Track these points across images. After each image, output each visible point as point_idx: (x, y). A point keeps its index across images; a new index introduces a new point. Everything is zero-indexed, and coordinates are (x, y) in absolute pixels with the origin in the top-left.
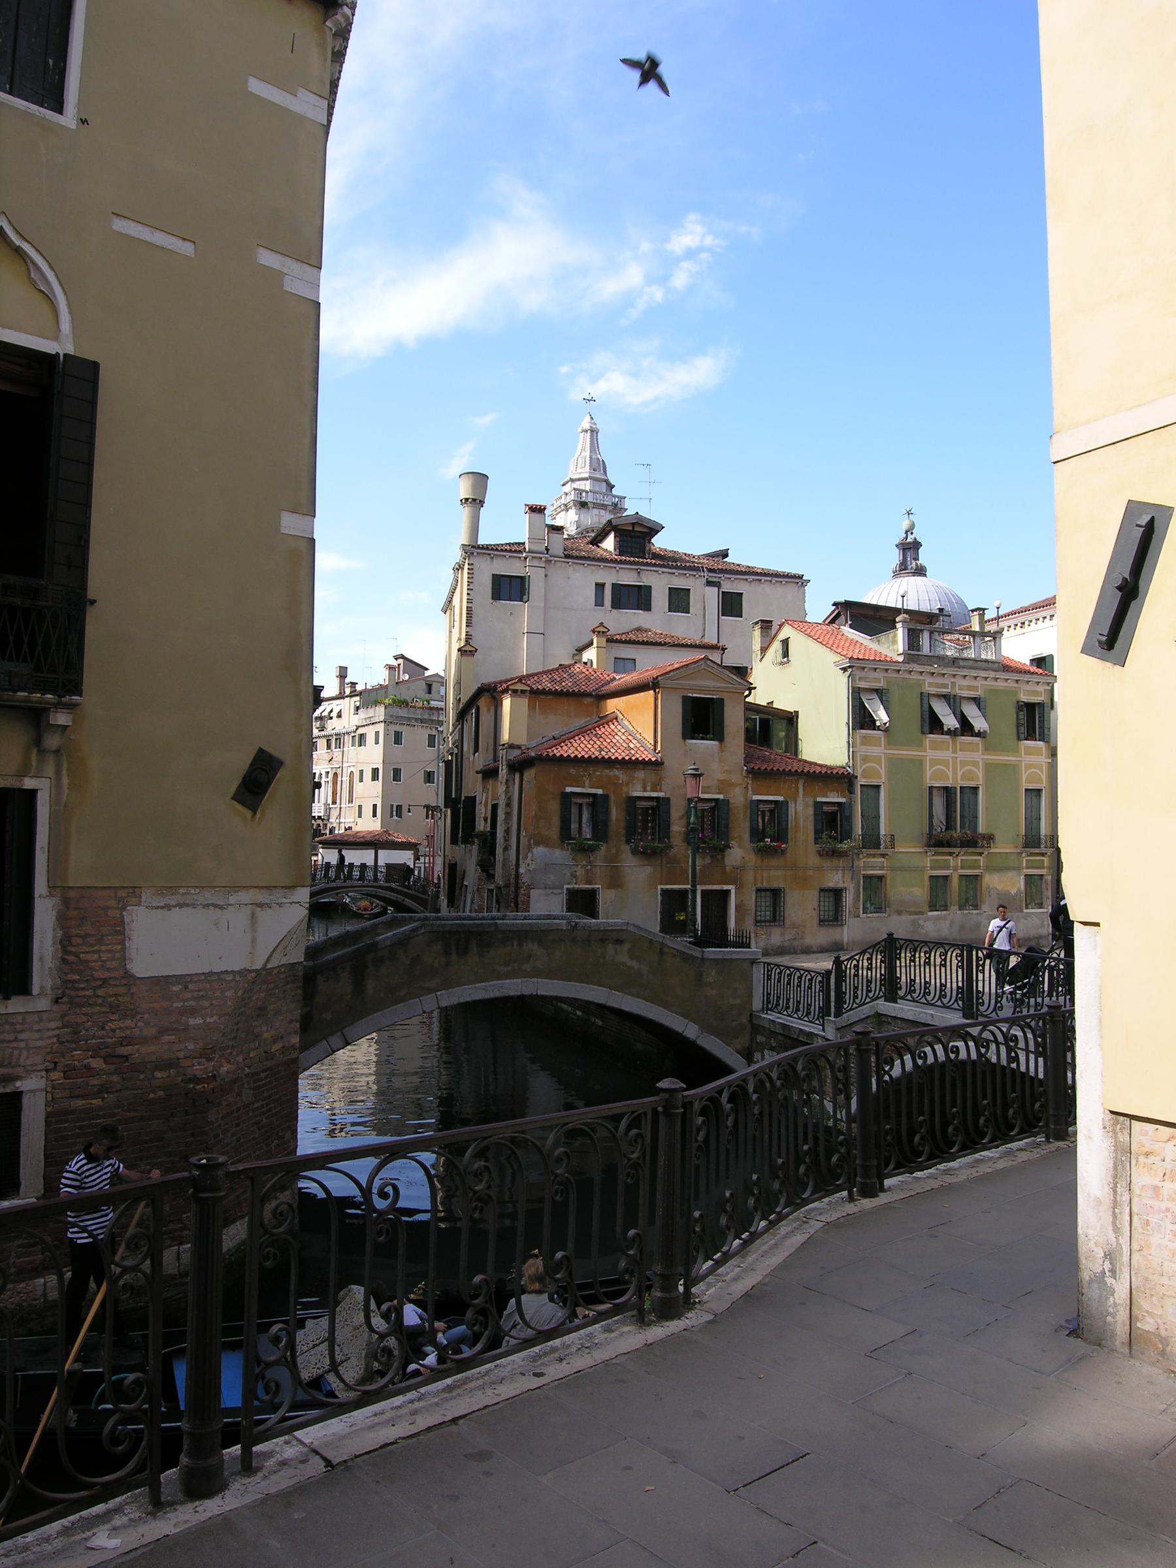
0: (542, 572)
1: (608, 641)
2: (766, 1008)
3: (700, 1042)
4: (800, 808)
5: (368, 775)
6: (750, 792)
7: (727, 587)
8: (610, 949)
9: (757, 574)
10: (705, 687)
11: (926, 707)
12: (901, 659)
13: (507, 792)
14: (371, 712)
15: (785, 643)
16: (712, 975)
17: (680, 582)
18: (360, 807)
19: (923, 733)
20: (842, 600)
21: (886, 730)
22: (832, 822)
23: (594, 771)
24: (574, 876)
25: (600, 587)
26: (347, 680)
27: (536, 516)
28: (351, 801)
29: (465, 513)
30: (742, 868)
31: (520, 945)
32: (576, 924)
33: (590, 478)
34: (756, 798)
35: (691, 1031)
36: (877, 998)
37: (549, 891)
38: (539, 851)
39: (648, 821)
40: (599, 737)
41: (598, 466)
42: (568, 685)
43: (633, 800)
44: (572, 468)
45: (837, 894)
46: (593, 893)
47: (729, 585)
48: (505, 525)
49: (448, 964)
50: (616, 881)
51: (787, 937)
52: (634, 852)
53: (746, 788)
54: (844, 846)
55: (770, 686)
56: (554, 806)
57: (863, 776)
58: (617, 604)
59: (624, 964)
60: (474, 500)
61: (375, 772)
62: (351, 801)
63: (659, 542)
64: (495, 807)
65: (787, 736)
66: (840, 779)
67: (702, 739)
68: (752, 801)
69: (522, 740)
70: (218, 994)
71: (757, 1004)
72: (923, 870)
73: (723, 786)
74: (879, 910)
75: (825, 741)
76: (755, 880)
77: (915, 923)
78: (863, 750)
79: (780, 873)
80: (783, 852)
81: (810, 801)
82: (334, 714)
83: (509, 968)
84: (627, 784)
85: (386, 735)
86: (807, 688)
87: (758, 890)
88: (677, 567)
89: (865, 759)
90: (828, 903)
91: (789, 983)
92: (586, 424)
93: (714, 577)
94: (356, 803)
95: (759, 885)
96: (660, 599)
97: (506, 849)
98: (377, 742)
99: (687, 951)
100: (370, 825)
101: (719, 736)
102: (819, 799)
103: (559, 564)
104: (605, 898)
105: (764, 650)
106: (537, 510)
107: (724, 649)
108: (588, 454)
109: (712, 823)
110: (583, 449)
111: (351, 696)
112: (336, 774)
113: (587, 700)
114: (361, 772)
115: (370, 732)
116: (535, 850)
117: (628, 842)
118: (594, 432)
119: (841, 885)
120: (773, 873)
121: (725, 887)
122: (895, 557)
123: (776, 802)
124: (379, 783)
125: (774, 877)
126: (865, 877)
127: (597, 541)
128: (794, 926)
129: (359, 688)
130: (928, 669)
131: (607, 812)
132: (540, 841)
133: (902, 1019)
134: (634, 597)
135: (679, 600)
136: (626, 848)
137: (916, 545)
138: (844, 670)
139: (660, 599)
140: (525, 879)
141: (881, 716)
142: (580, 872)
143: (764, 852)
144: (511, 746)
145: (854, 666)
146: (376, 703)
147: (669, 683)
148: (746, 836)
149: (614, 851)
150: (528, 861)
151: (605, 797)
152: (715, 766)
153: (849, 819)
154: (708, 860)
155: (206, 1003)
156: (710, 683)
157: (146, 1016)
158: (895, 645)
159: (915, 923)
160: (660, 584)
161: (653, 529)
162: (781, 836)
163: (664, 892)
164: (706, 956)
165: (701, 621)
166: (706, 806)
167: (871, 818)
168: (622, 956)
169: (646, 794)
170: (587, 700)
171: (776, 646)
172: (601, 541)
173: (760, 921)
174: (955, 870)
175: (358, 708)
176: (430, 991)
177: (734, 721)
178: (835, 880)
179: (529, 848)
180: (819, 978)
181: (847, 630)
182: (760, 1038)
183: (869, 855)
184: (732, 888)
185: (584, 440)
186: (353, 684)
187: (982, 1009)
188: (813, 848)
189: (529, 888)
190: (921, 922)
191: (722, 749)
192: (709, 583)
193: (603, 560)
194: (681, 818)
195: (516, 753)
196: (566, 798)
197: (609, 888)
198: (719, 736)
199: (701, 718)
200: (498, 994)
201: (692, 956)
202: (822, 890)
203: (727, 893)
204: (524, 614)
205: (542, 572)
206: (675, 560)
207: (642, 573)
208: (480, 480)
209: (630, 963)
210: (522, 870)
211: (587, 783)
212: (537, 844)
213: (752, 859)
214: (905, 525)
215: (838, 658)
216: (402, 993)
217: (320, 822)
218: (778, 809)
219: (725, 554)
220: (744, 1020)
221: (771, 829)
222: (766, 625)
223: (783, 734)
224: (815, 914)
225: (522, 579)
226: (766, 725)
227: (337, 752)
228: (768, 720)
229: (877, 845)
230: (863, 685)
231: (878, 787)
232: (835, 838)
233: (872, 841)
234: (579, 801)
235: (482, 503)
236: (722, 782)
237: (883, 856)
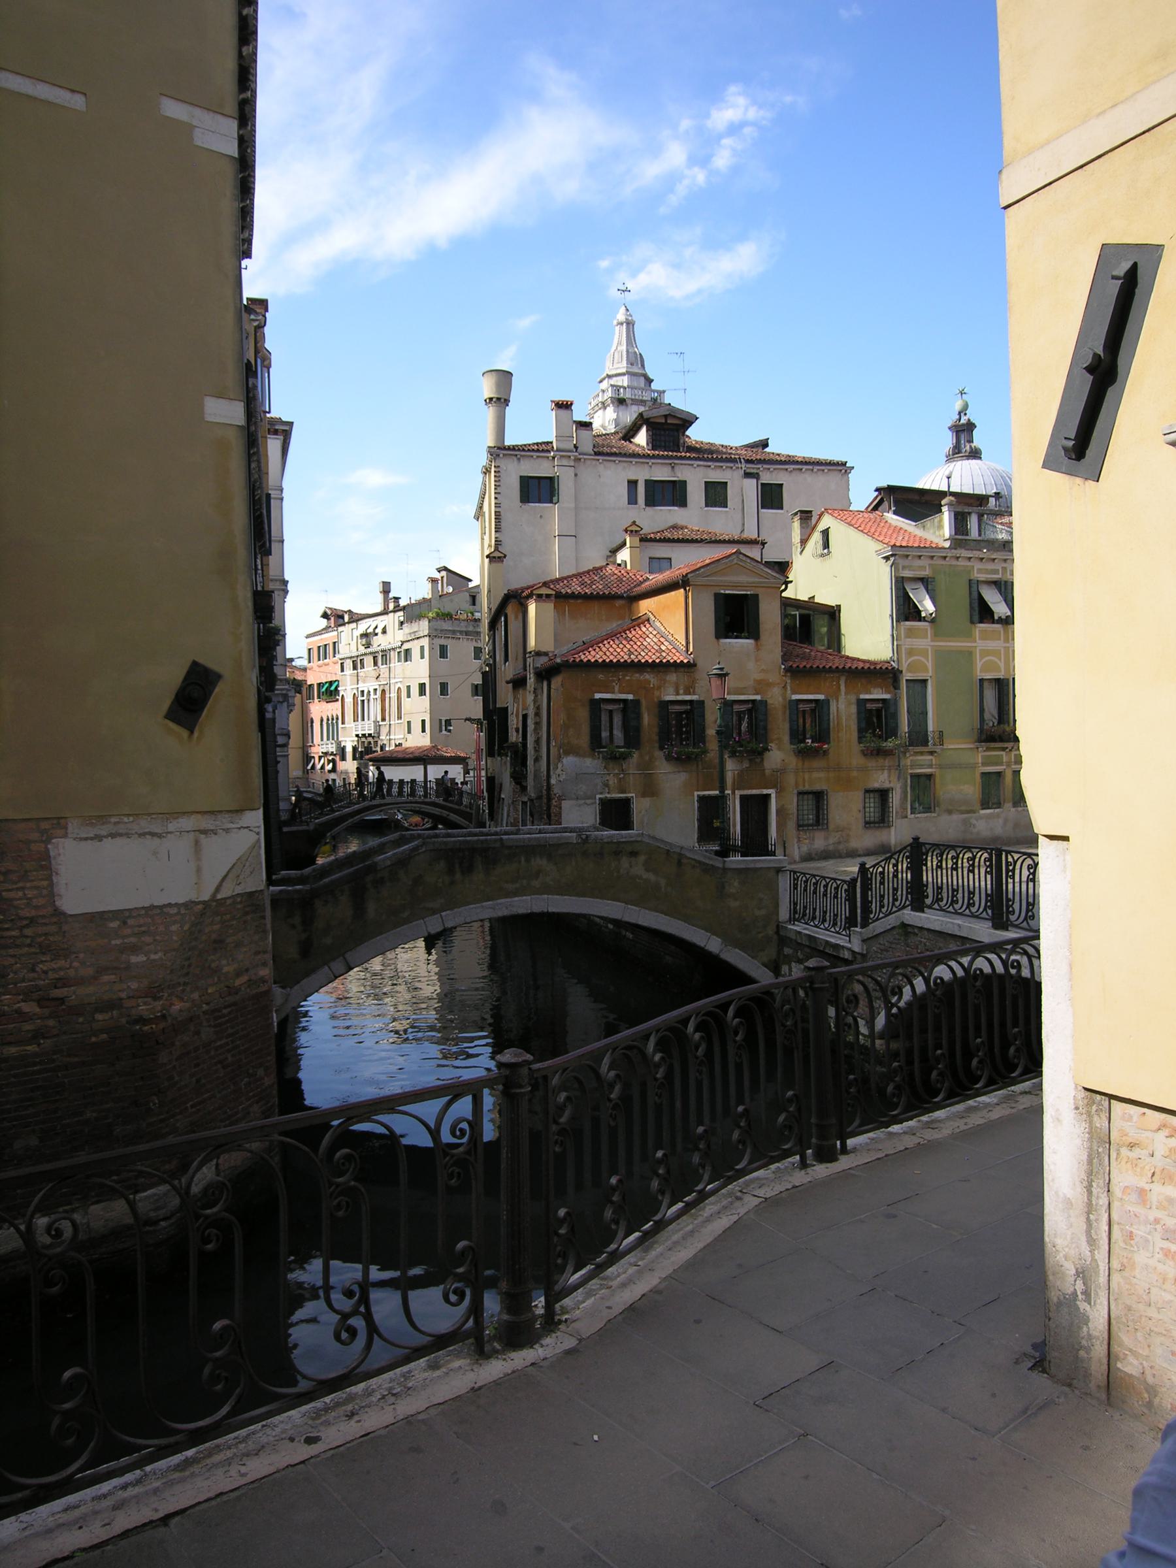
0: (571, 471)
1: (641, 540)
2: (792, 920)
3: (724, 956)
4: (842, 706)
5: (415, 690)
6: (789, 692)
7: (767, 478)
8: (625, 862)
9: (797, 463)
10: (738, 583)
11: (975, 595)
12: (947, 545)
13: (535, 701)
14: (415, 627)
15: (826, 533)
16: (734, 886)
17: (716, 476)
18: (409, 723)
19: (972, 622)
20: (885, 484)
21: (933, 621)
22: (876, 722)
23: (624, 676)
24: (607, 785)
25: (632, 484)
26: (391, 595)
27: (563, 412)
28: (400, 718)
29: (490, 413)
30: (783, 771)
31: (528, 861)
32: (587, 836)
33: (628, 373)
34: (795, 697)
35: (713, 945)
36: (904, 907)
38: (569, 761)
39: (682, 726)
40: (629, 640)
41: (636, 359)
42: (599, 587)
44: (608, 364)
45: (883, 795)
46: (627, 802)
47: (768, 475)
48: (531, 424)
49: (452, 883)
50: (650, 789)
51: (831, 841)
52: (669, 758)
53: (785, 687)
54: (889, 744)
55: (808, 580)
56: (583, 714)
57: (909, 670)
58: (651, 502)
60: (499, 399)
61: (422, 687)
62: (400, 718)
63: (696, 434)
64: (525, 717)
65: (830, 632)
66: (884, 674)
67: (737, 637)
68: (791, 701)
69: (549, 647)
70: (161, 928)
71: (784, 914)
72: (973, 767)
73: (761, 686)
74: (928, 809)
75: (868, 636)
76: (797, 785)
77: (965, 822)
78: (908, 643)
79: (822, 775)
80: (826, 753)
81: (853, 698)
82: (379, 631)
83: (518, 885)
84: (659, 688)
85: (431, 649)
86: (847, 578)
87: (799, 793)
88: (712, 460)
89: (910, 652)
90: (873, 804)
91: (815, 892)
92: (621, 316)
93: (752, 468)
94: (405, 719)
95: (801, 788)
96: (696, 494)
97: (537, 760)
98: (422, 657)
99: (707, 861)
100: (419, 740)
101: (755, 634)
102: (862, 696)
103: (588, 462)
104: (640, 807)
105: (804, 542)
106: (564, 406)
107: (763, 544)
108: (624, 348)
109: (748, 726)
110: (619, 343)
111: (394, 611)
112: (383, 691)
113: (619, 602)
114: (409, 687)
115: (415, 647)
116: (564, 760)
117: (661, 748)
118: (630, 324)
119: (887, 785)
120: (815, 775)
121: (765, 792)
122: (948, 440)
123: (817, 701)
124: (426, 699)
125: (817, 779)
126: (912, 776)
127: (629, 434)
128: (838, 829)
129: (402, 603)
130: (977, 554)
131: (639, 717)
132: (570, 750)
133: (929, 930)
134: (669, 493)
135: (716, 494)
136: (659, 754)
137: (970, 426)
138: (887, 558)
139: (696, 494)
140: (556, 790)
141: (927, 606)
142: (613, 781)
143: (804, 754)
144: (538, 654)
145: (898, 555)
146: (420, 617)
147: (701, 580)
148: (786, 738)
149: (647, 758)
150: (559, 771)
151: (636, 703)
152: (751, 665)
153: (895, 716)
154: (746, 764)
155: (148, 939)
156: (743, 579)
157: (81, 955)
158: (940, 530)
159: (965, 822)
160: (695, 477)
161: (687, 421)
162: (823, 736)
163: (702, 799)
164: (728, 865)
165: (740, 515)
166: (743, 708)
167: (919, 715)
168: (638, 869)
169: (679, 698)
170: (619, 602)
171: (817, 537)
172: (633, 436)
173: (803, 826)
174: (1008, 765)
175: (402, 623)
176: (434, 912)
177: (770, 617)
178: (881, 779)
179: (559, 758)
180: (845, 887)
181: (891, 517)
182: (787, 951)
183: (916, 753)
184: (772, 792)
185: (620, 333)
186: (396, 599)
187: (1012, 918)
188: (856, 748)
189: (560, 799)
190: (973, 821)
191: (758, 648)
192: (748, 475)
193: (634, 455)
195: (543, 660)
196: (595, 705)
197: (644, 795)
198: (755, 634)
199: (735, 615)
202: (867, 791)
203: (768, 796)
204: (554, 516)
205: (571, 471)
206: (711, 452)
207: (677, 468)
208: (504, 378)
209: (645, 876)
210: (553, 781)
211: (617, 688)
212: (567, 753)
213: (793, 761)
214: (958, 405)
215: (879, 546)
216: (406, 914)
217: (370, 739)
218: (819, 709)
219: (764, 444)
220: (771, 931)
221: (811, 730)
222: (805, 516)
223: (824, 630)
224: (860, 815)
225: (551, 479)
226: (806, 621)
227: (383, 668)
228: (808, 616)
229: (925, 743)
230: (907, 574)
231: (925, 681)
232: (880, 737)
233: (919, 738)
234: (610, 707)
235: (507, 402)
236: (759, 682)
237: (931, 753)
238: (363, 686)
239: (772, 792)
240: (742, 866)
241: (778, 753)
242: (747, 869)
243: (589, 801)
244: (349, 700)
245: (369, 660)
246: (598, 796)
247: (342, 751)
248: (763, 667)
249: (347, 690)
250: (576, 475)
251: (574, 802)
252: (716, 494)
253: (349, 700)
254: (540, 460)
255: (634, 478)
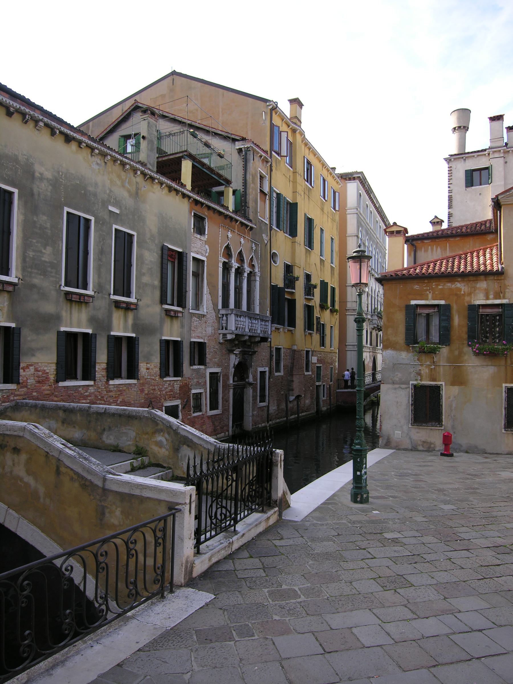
0: (501, 160)
23: (437, 285)
24: (419, 374)
27: (496, 123)
37: (397, 386)
39: (495, 326)
43: (473, 309)
50: (458, 379)
52: (478, 354)
56: (400, 317)
60: (459, 127)
84: (470, 294)
104: (449, 394)
136: (468, 350)
142: (425, 371)
149: (456, 353)
169: (489, 302)
197: (454, 383)
201: (90, 481)
205: (501, 160)
211: (430, 296)
234: (427, 311)
242: (131, 496)
243: (403, 386)
246: (411, 382)
250: (506, 162)
251: (390, 386)
254: (480, 157)
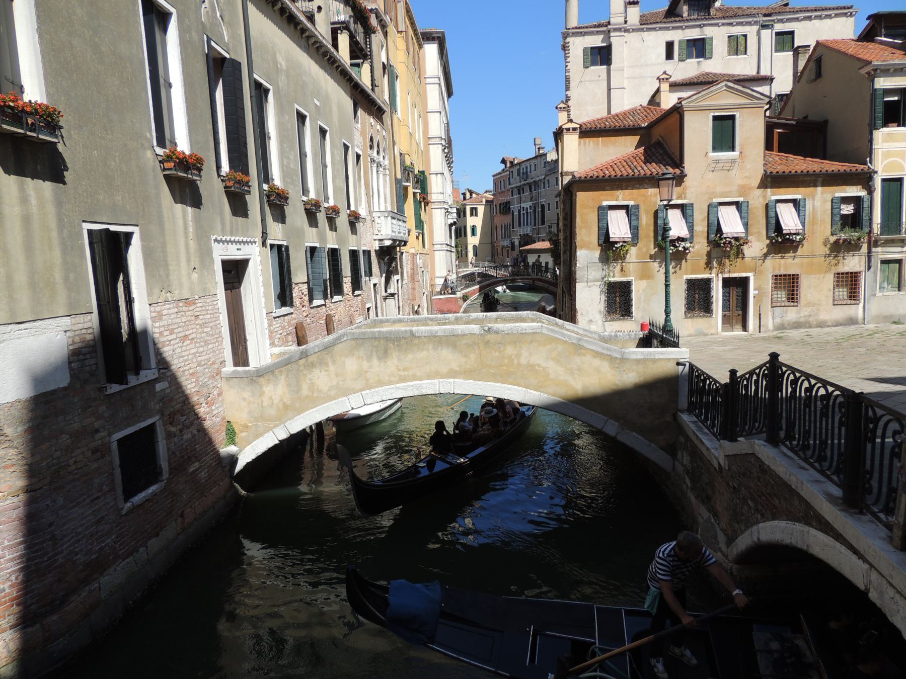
2: (690, 410)
3: (620, 438)
4: (818, 203)
7: (779, 27)
17: (738, 30)
25: (670, 46)
28: (543, 223)
37: (590, 284)
59: (539, 365)
94: (547, 224)
121: (744, 275)
128: (809, 304)
164: (626, 356)
194: (703, 220)
200: (416, 393)
219: (787, 5)
238: (523, 205)
239: (750, 275)
240: (639, 357)
241: (757, 243)
244: (516, 213)
245: (527, 188)
247: (513, 244)
248: (747, 174)
249: (515, 207)
252: (737, 46)
253: (516, 213)
255: (670, 39)
